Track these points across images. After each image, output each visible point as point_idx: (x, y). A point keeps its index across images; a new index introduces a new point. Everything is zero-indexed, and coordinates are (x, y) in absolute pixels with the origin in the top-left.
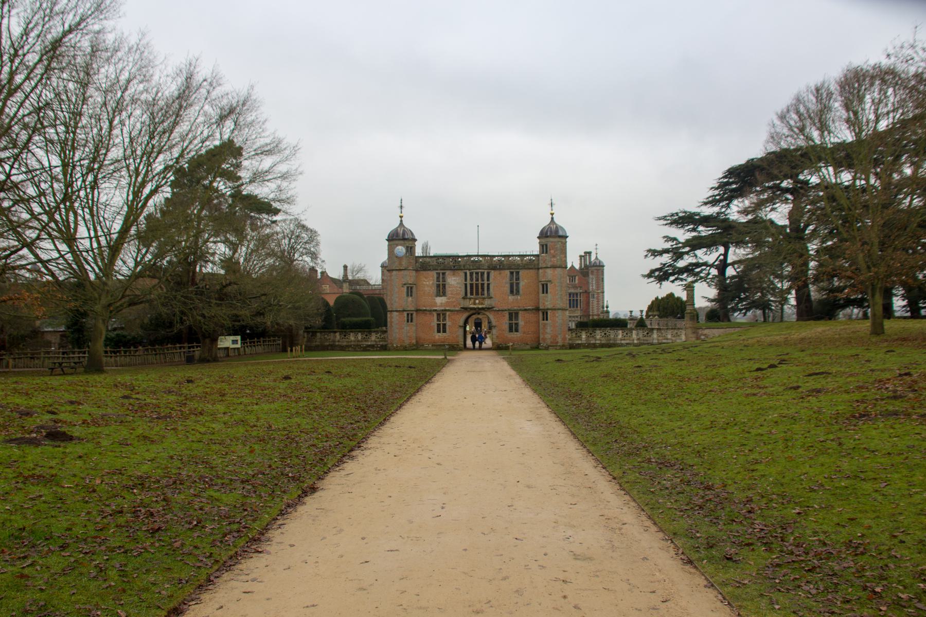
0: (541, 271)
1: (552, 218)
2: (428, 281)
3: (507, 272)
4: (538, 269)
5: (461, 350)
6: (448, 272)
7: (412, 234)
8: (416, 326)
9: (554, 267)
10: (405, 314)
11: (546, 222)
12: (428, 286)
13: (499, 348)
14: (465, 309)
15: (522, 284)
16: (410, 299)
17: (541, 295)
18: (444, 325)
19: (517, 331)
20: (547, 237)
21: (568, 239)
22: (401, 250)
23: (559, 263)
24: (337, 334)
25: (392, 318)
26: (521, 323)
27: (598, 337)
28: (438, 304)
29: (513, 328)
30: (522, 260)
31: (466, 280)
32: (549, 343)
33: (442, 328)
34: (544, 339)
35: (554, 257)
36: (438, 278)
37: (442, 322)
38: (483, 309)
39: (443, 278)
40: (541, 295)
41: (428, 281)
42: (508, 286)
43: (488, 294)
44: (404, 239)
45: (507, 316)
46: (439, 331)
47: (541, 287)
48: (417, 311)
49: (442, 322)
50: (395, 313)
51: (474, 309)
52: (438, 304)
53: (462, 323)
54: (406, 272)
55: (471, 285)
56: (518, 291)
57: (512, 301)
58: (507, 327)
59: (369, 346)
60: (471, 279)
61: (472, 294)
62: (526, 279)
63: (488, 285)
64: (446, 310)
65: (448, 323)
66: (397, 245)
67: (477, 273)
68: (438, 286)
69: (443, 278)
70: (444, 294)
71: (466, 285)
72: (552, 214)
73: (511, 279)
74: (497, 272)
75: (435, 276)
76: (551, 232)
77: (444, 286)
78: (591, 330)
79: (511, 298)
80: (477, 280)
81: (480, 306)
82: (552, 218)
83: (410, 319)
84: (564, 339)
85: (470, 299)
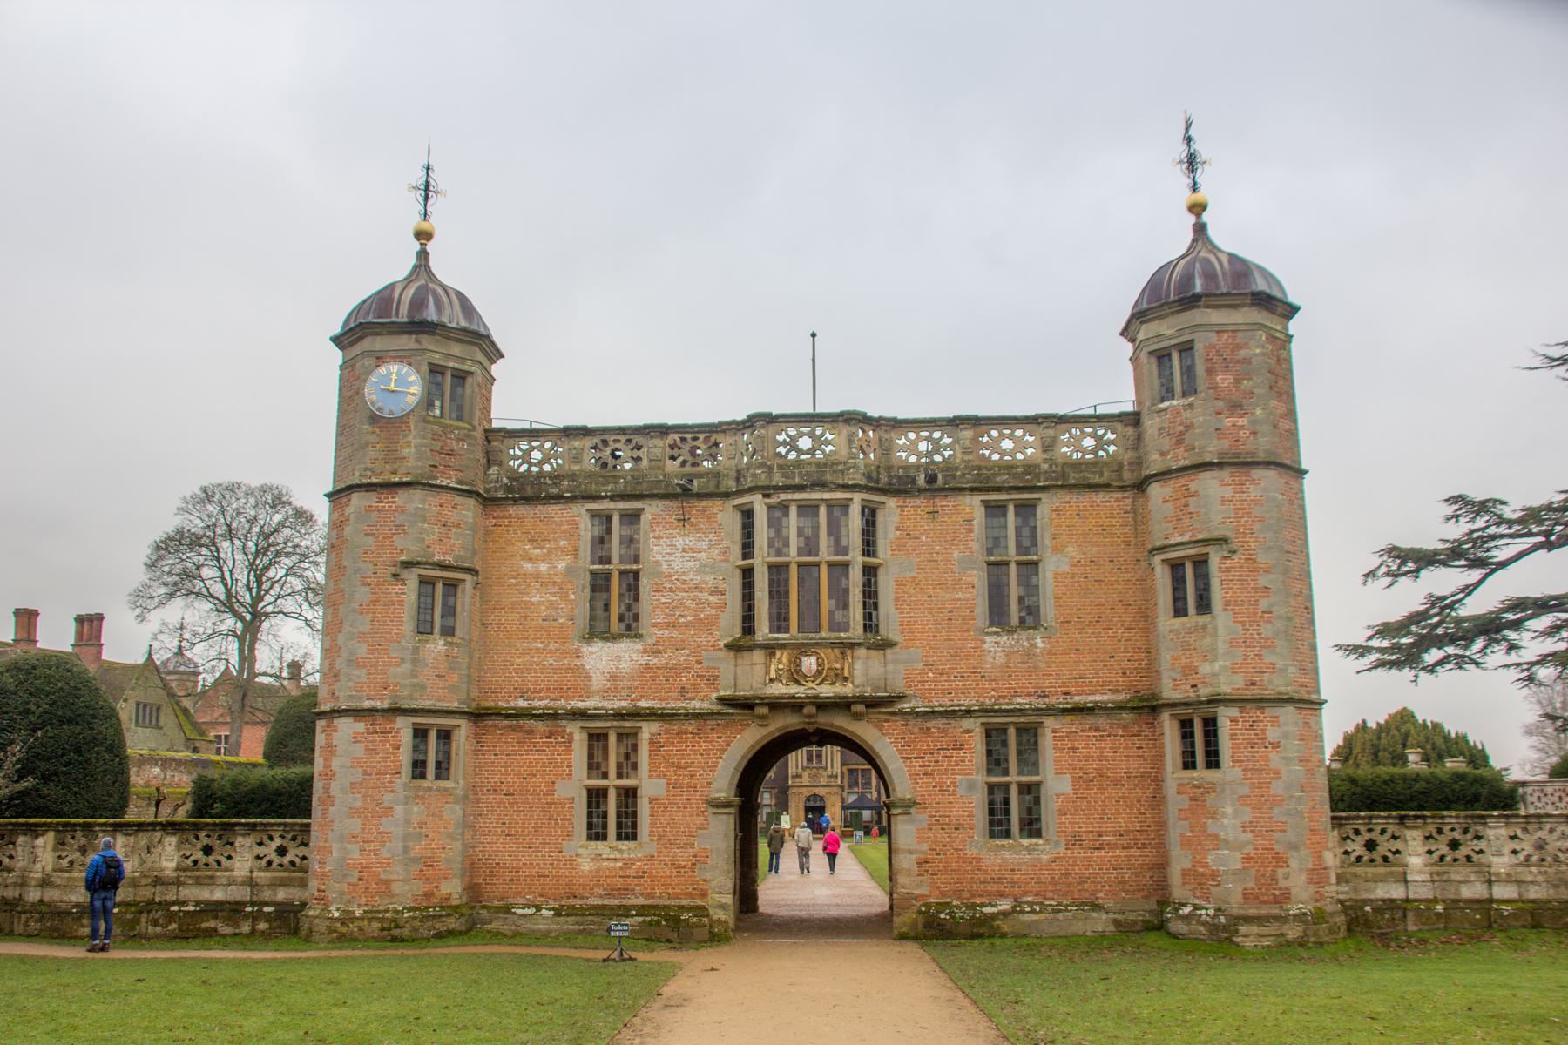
0: (1156, 490)
1: (1200, 229)
2: (546, 560)
3: (973, 505)
4: (1140, 486)
5: (716, 938)
6: (651, 510)
7: (467, 308)
8: (471, 797)
9: (1240, 463)
10: (404, 729)
11: (1175, 242)
12: (544, 582)
13: (936, 927)
14: (745, 705)
15: (1053, 567)
16: (438, 645)
17: (1166, 622)
18: (630, 794)
19: (1032, 826)
20: (1189, 301)
21: (1293, 326)
22: (399, 383)
23: (1263, 445)
24: (46, 842)
25: (331, 750)
26: (1056, 784)
27: (1501, 863)
28: (598, 681)
29: (1016, 812)
30: (1048, 446)
31: (747, 549)
32: (1236, 905)
33: (611, 814)
34: (1201, 879)
35: (1235, 407)
36: (601, 541)
37: (613, 781)
38: (842, 705)
39: (629, 541)
40: (1166, 622)
41: (546, 560)
42: (978, 578)
43: (870, 625)
44: (419, 327)
45: (977, 743)
46: (596, 833)
47: (1162, 577)
48: (478, 716)
49: (613, 781)
50: (346, 726)
51: (795, 705)
52: (598, 681)
53: (723, 781)
54: (412, 501)
55: (778, 571)
56: (1031, 617)
57: (1000, 665)
58: (976, 805)
59: (212, 909)
60: (778, 542)
61: (780, 621)
62: (1070, 543)
63: (870, 572)
64: (635, 714)
65: (650, 786)
66: (380, 359)
67: (808, 509)
68: (599, 583)
69: (629, 541)
70: (630, 627)
71: (748, 573)
72: (1197, 208)
73: (995, 543)
74: (917, 507)
75: (587, 530)
76: (1210, 276)
77: (632, 581)
78: (1453, 818)
79: (996, 646)
80: (810, 547)
81: (826, 691)
82: (1200, 229)
83: (430, 757)
84: (1317, 875)
85: (770, 648)
